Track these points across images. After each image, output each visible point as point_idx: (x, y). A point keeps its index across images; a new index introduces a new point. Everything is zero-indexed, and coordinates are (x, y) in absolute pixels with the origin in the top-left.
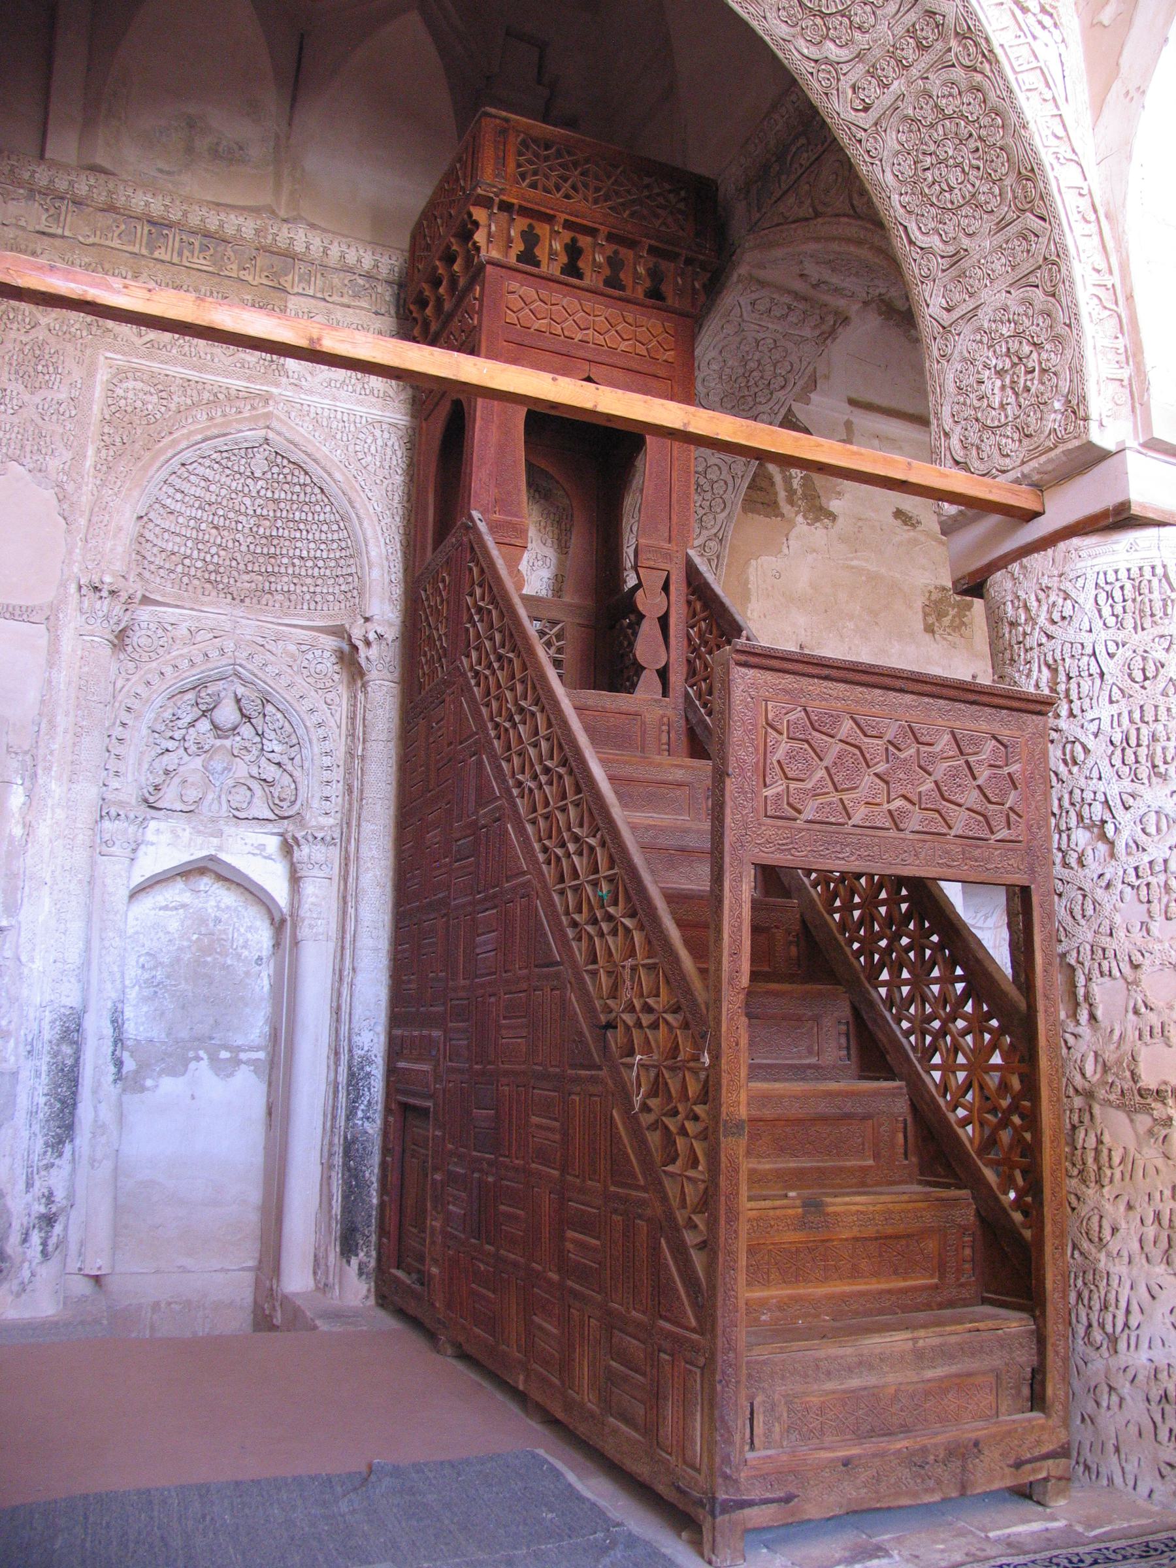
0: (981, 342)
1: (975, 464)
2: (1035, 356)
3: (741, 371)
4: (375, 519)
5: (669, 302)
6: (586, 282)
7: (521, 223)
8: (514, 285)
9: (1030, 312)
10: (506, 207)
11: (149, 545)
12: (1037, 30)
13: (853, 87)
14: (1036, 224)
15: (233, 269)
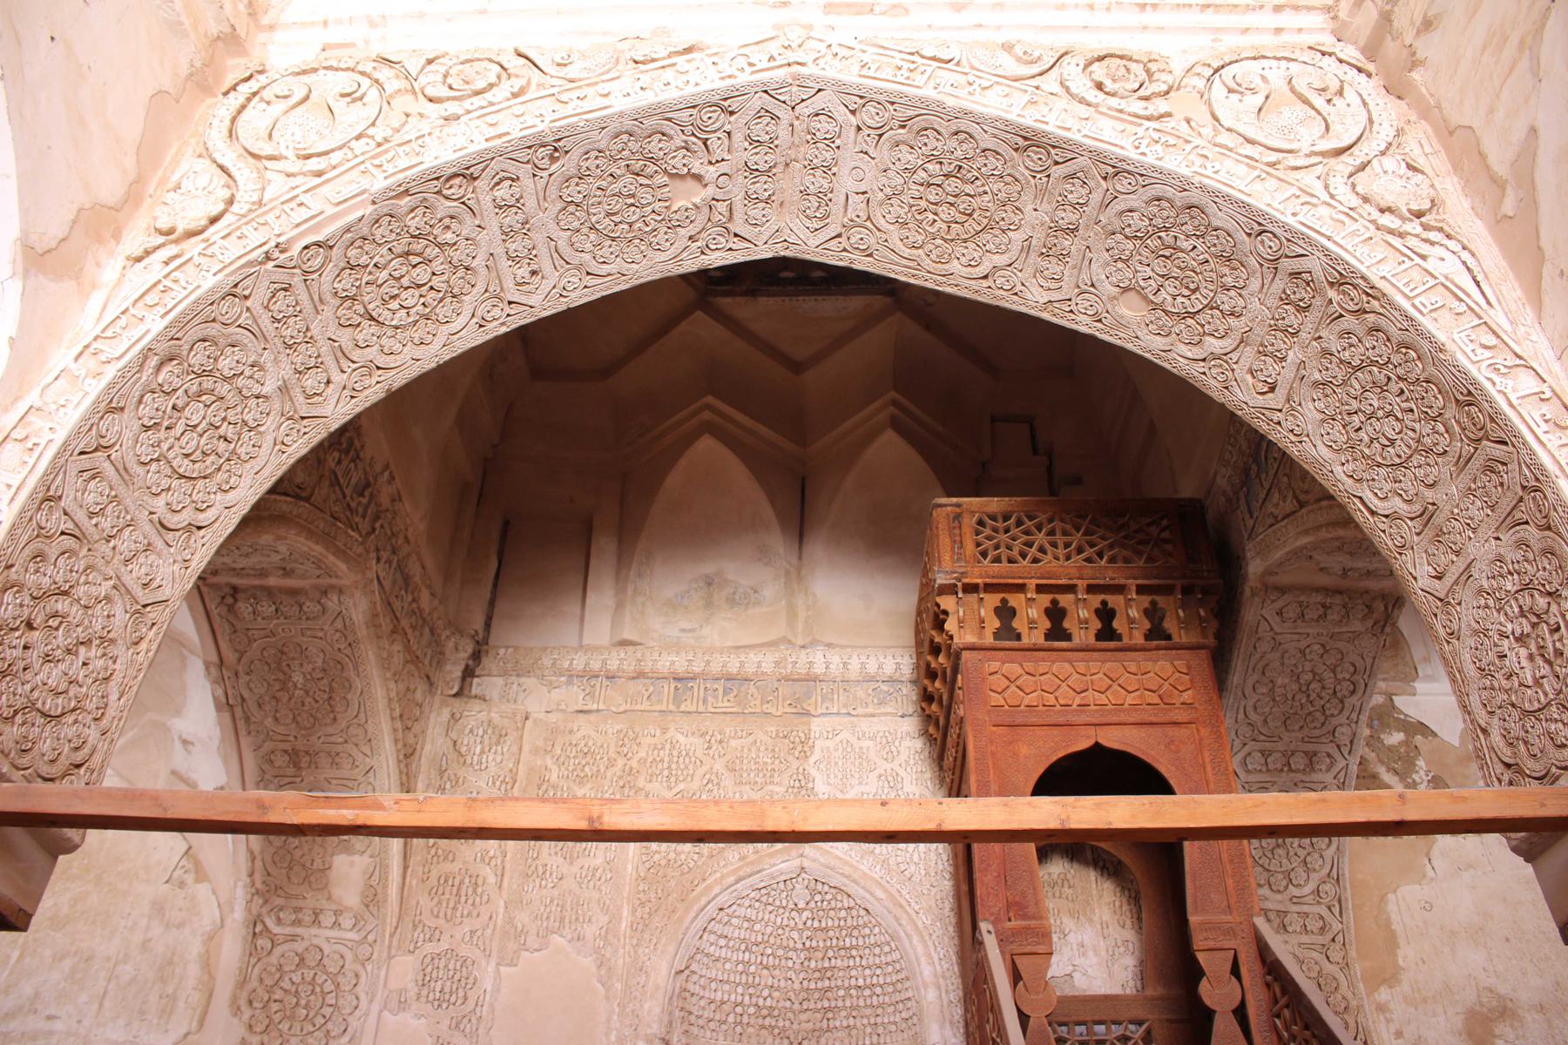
0: (1487, 607)
1: (1530, 766)
2: (1554, 608)
3: (1295, 687)
4: (925, 934)
5: (1176, 639)
6: (1076, 641)
7: (993, 600)
8: (995, 665)
9: (1531, 556)
10: (971, 589)
11: (694, 999)
12: (1425, 249)
13: (1251, 372)
14: (1498, 451)
15: (755, 705)
